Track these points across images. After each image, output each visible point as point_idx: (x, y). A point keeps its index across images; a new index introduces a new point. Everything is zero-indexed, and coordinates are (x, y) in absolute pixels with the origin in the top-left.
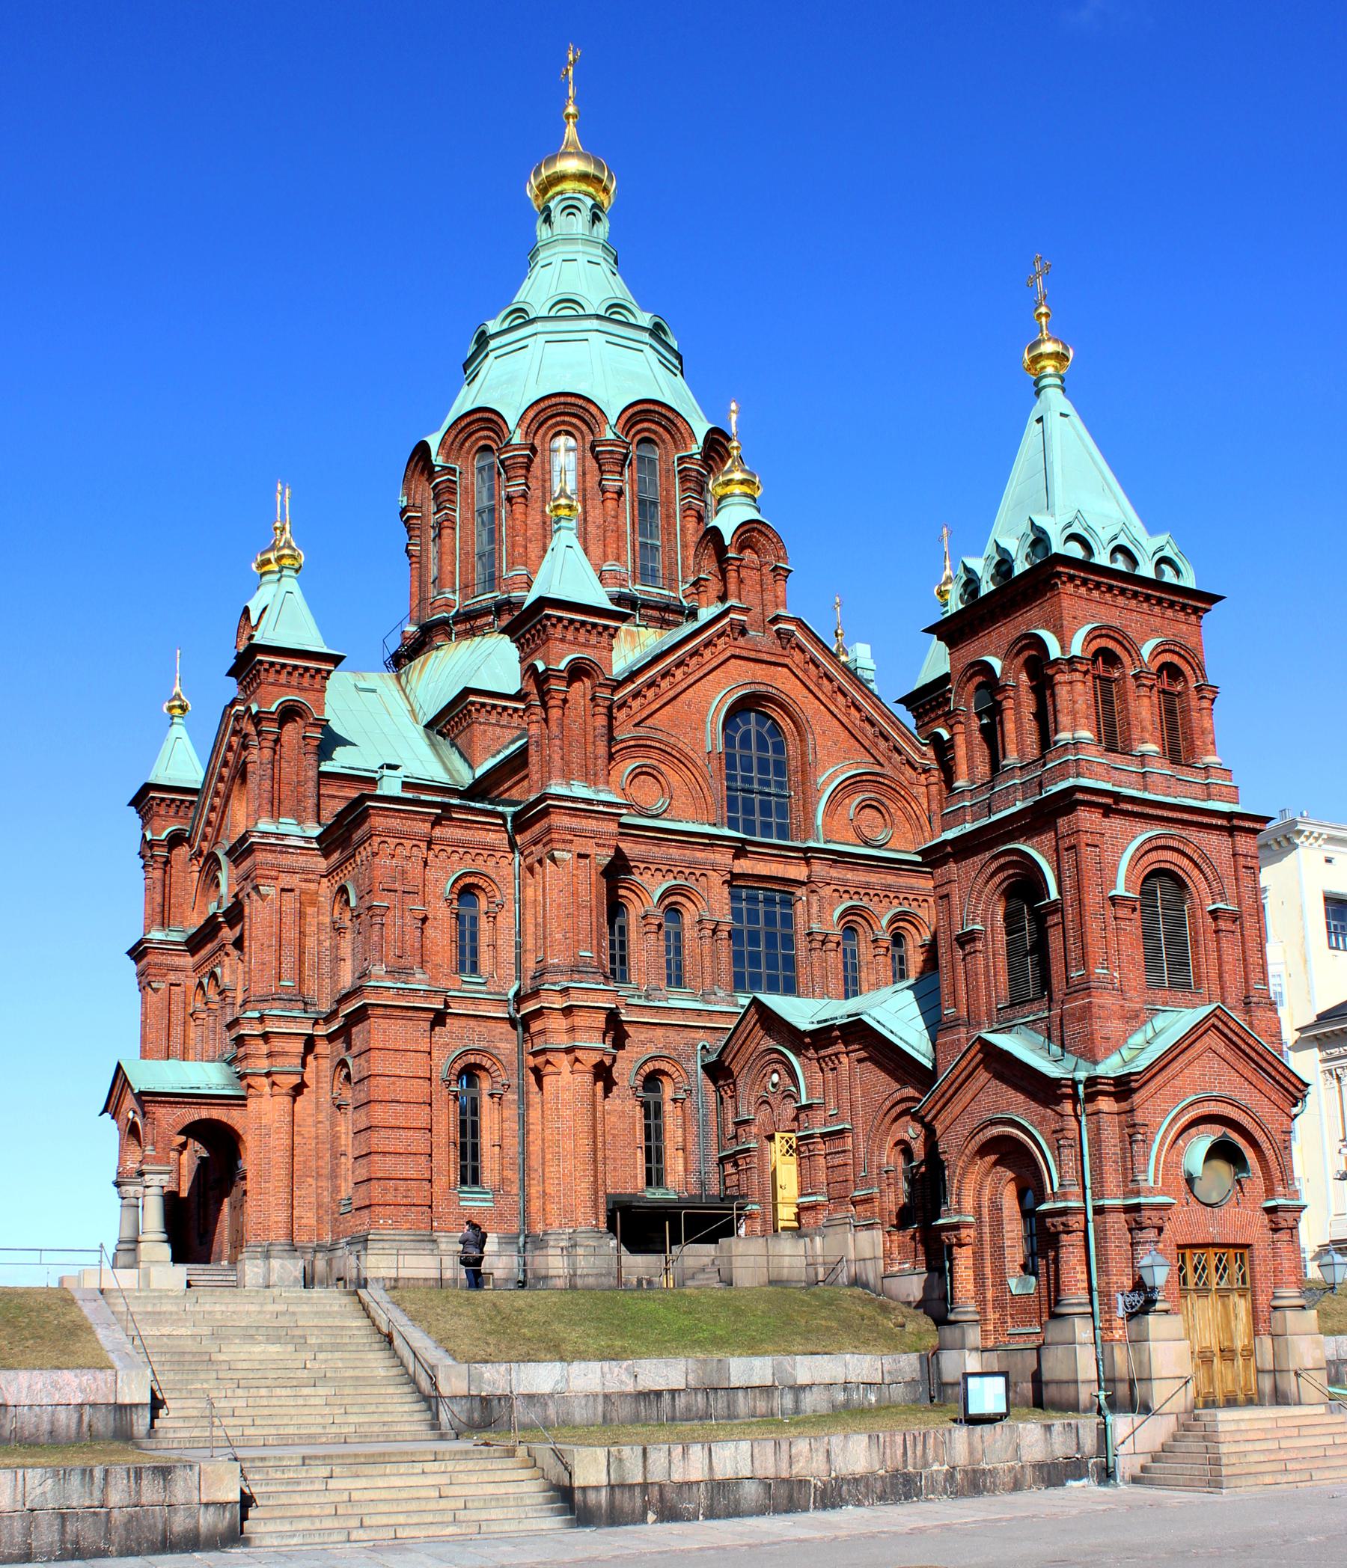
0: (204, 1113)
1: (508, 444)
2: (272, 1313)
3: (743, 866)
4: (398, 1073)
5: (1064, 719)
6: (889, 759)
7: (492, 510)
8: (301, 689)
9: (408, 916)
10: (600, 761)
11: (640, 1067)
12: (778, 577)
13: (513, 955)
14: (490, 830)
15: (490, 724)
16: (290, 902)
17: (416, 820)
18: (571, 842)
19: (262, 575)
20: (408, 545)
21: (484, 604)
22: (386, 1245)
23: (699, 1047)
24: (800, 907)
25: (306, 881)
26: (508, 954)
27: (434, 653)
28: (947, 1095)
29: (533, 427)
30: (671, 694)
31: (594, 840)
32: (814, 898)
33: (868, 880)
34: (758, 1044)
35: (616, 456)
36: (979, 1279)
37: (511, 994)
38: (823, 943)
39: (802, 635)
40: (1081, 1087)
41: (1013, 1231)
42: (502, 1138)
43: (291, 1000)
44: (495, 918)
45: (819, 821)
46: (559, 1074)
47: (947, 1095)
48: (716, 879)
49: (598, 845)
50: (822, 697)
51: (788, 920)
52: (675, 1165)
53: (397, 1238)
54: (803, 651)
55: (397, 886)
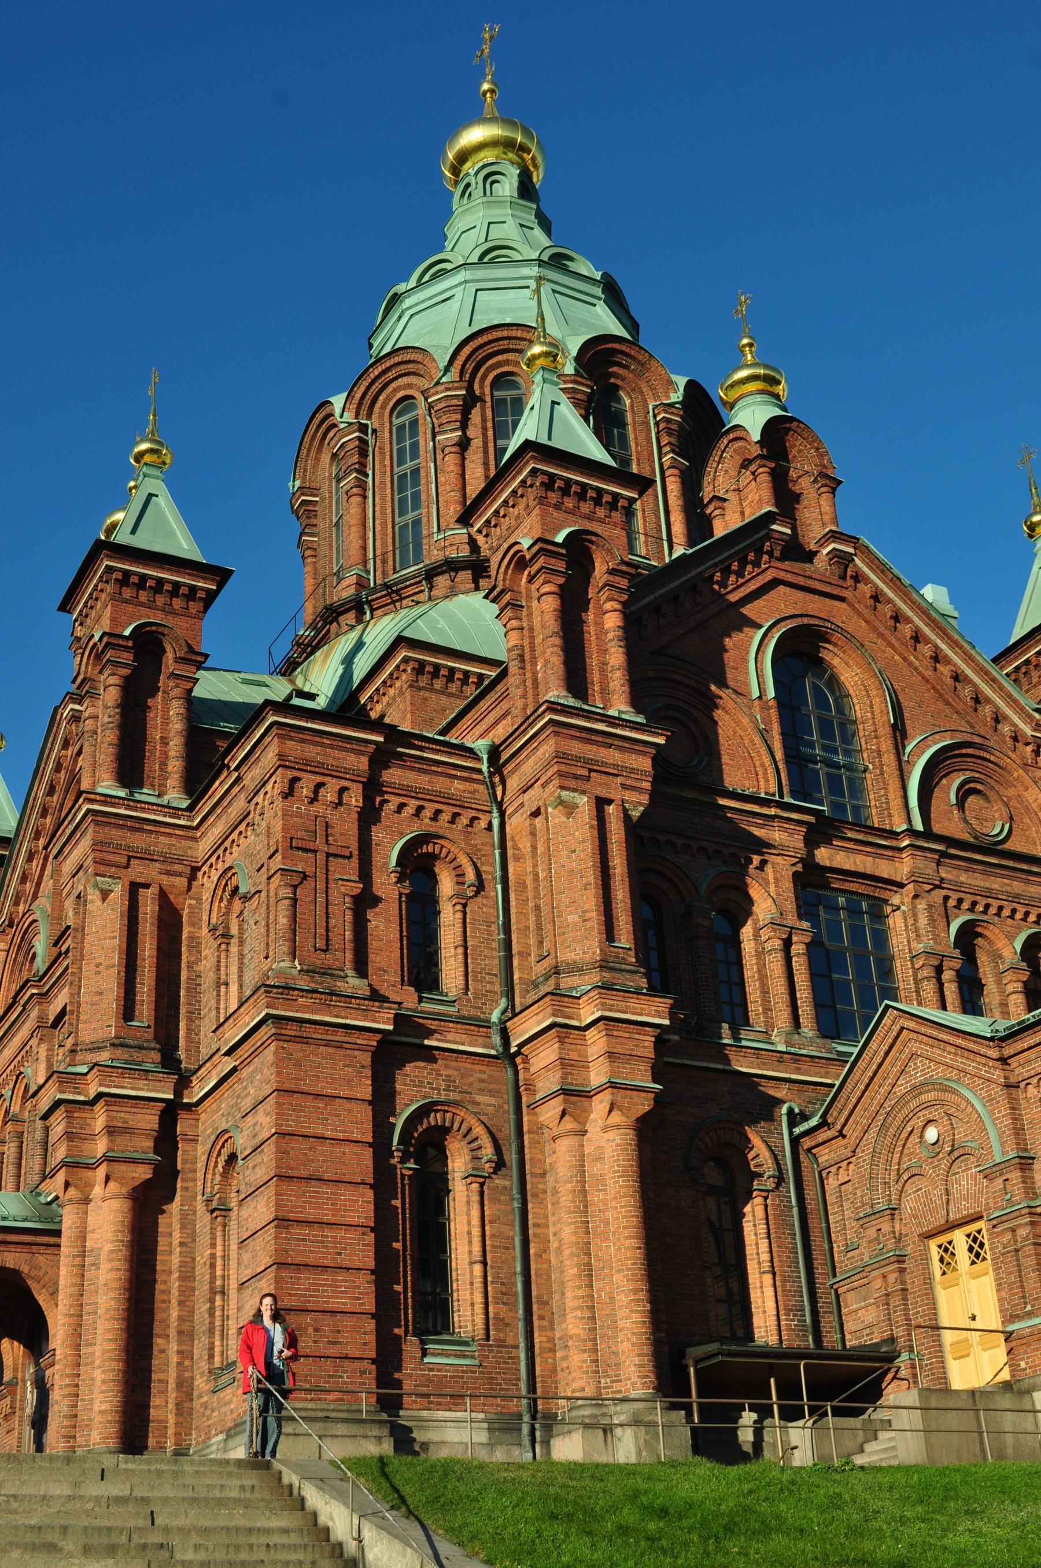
2: (97, 1499)
4: (320, 1131)
7: (416, 472)
12: (823, 489)
14: (455, 777)
15: (432, 690)
17: (345, 749)
20: (302, 534)
24: (896, 922)
25: (168, 873)
29: (470, 367)
31: (619, 780)
33: (987, 885)
35: (578, 396)
37: (495, 1017)
39: (863, 561)
44: (465, 905)
49: (624, 786)
50: (897, 644)
51: (881, 938)
55: (319, 843)
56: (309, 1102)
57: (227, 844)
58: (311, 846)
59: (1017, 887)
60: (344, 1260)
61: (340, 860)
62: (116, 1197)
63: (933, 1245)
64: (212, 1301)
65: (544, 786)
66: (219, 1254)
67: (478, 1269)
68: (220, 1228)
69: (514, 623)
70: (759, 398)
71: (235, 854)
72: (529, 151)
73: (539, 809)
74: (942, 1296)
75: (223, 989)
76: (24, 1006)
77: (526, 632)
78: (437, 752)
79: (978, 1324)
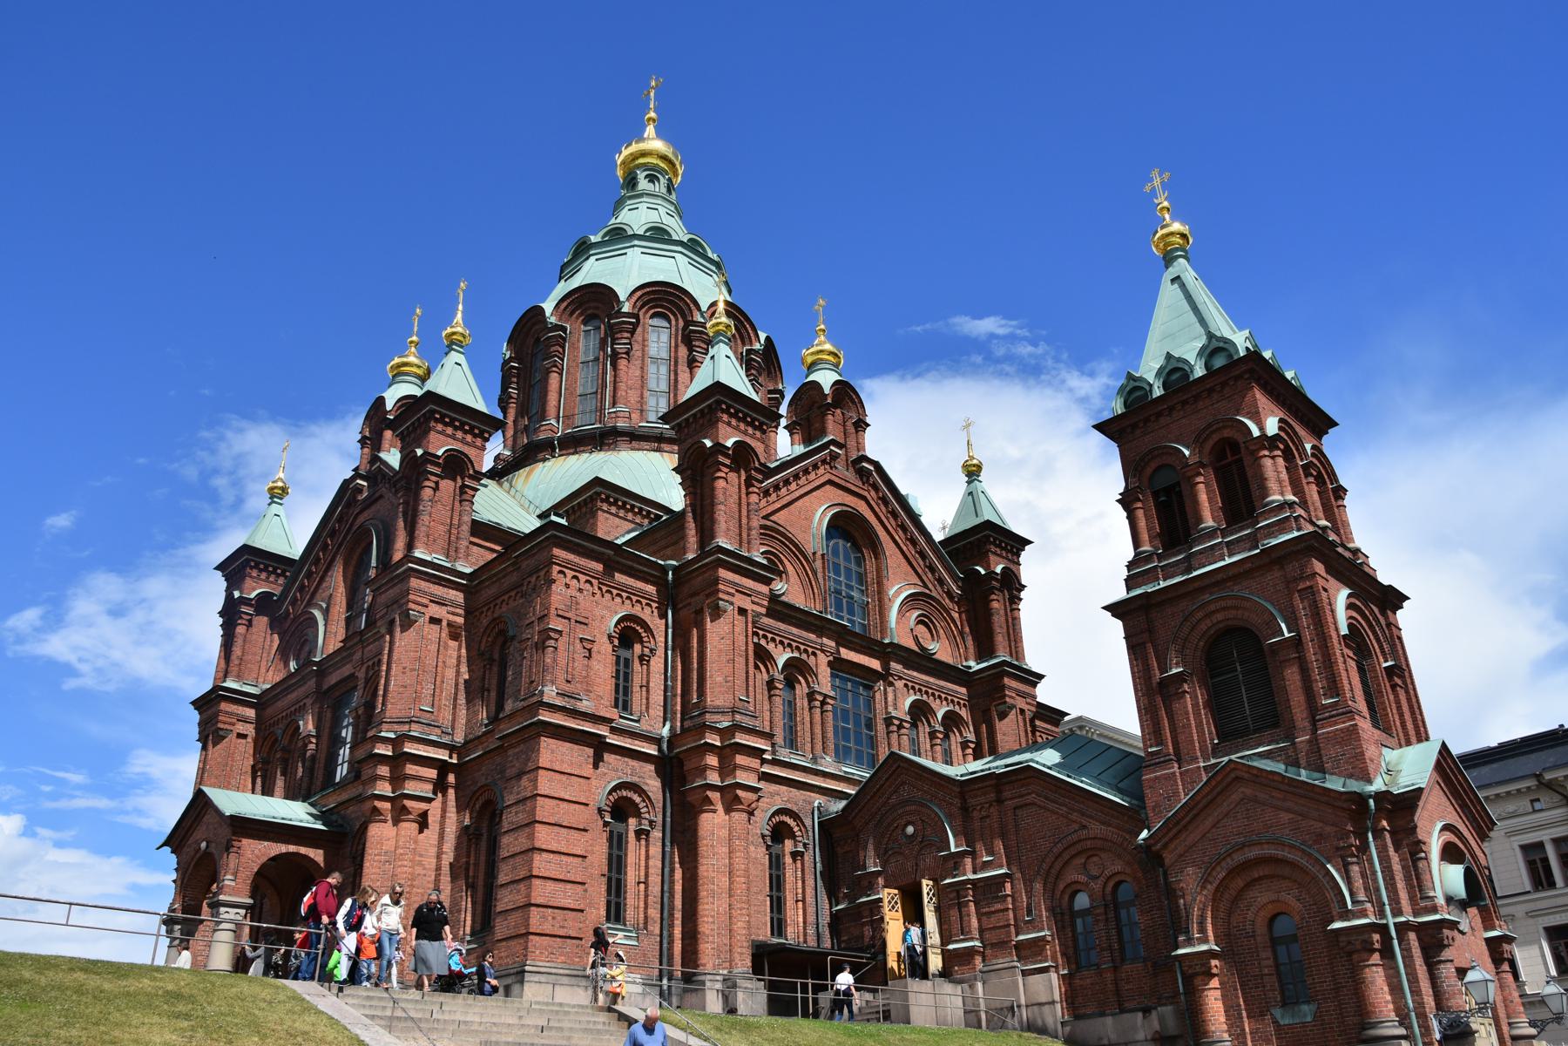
1: (619, 314)
4: (562, 795)
8: (463, 441)
9: (578, 645)
10: (754, 532)
11: (770, 819)
18: (733, 595)
22: (543, 978)
23: (816, 804)
25: (453, 614)
26: (657, 697)
27: (540, 465)
29: (639, 304)
30: (789, 499)
32: (890, 689)
34: (889, 798)
40: (1371, 802)
41: (1268, 959)
42: (647, 875)
43: (430, 725)
44: (648, 661)
46: (714, 811)
48: (823, 660)
49: (753, 602)
52: (794, 915)
53: (554, 971)
57: (499, 601)
58: (566, 615)
61: (582, 626)
65: (708, 596)
66: (472, 862)
67: (642, 886)
68: (473, 846)
69: (691, 489)
71: (504, 609)
75: (486, 693)
76: (303, 678)
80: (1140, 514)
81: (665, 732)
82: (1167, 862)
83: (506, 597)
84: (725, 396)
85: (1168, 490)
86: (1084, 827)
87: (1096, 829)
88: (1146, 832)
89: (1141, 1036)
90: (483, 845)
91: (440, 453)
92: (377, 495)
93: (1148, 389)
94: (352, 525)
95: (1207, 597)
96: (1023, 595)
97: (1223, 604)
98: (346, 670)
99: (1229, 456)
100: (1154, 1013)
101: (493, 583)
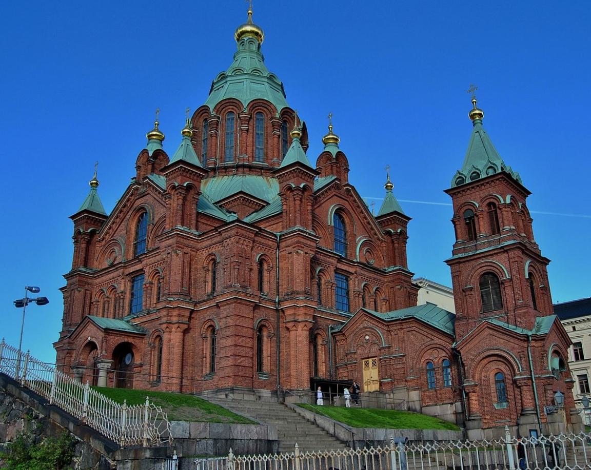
0: (126, 340)
3: (339, 266)
5: (506, 222)
6: (373, 237)
13: (275, 286)
15: (246, 205)
16: (187, 260)
17: (250, 232)
18: (303, 248)
19: (149, 140)
21: (229, 165)
24: (351, 282)
26: (274, 286)
28: (468, 341)
32: (357, 279)
36: (481, 404)
38: (359, 295)
45: (358, 254)
47: (468, 341)
48: (332, 269)
49: (311, 250)
54: (353, 197)
55: (243, 255)
56: (241, 318)
59: (375, 276)
60: (247, 355)
62: (180, 332)
63: (363, 361)
64: (203, 359)
67: (269, 358)
70: (334, 144)
71: (214, 250)
72: (261, 37)
73: (291, 253)
74: (364, 372)
76: (117, 268)
77: (288, 206)
78: (267, 234)
79: (372, 379)
80: (458, 226)
81: (277, 300)
82: (462, 354)
83: (215, 246)
84: (301, 167)
85: (470, 219)
86: (433, 340)
87: (437, 341)
88: (455, 343)
89: (449, 412)
90: (209, 341)
91: (185, 185)
92: (146, 193)
93: (464, 178)
94: (133, 204)
95: (481, 261)
96: (407, 240)
97: (487, 264)
98: (138, 267)
99: (492, 207)
100: (454, 404)
101: (209, 239)
